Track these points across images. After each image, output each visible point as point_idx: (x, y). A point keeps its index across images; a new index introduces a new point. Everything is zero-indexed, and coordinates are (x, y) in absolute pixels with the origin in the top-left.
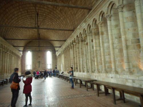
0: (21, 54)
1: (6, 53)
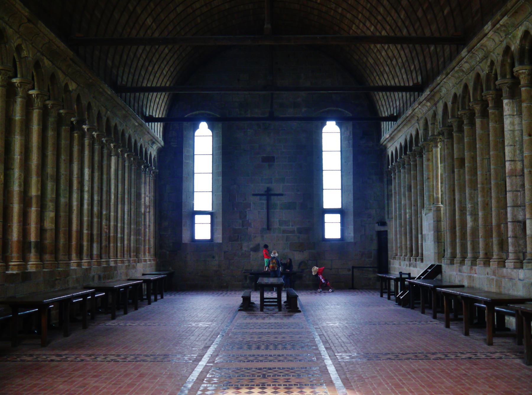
0: (153, 141)
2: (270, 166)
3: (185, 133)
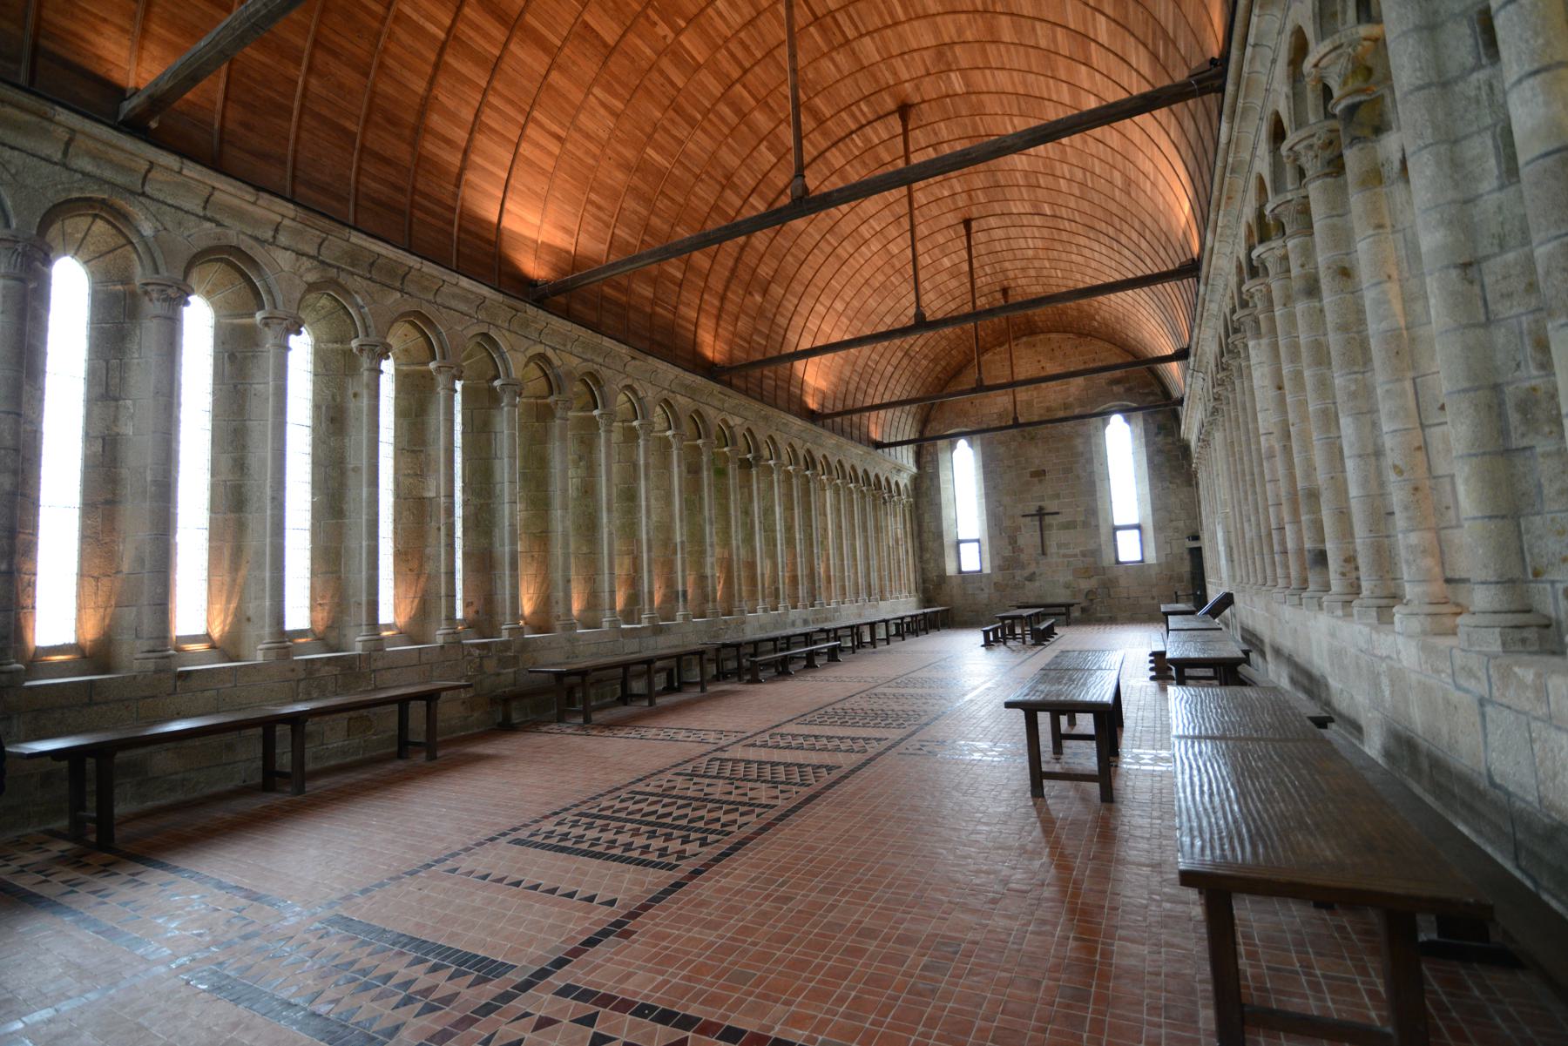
1: (754, 471)
2: (1040, 481)
3: (941, 456)
